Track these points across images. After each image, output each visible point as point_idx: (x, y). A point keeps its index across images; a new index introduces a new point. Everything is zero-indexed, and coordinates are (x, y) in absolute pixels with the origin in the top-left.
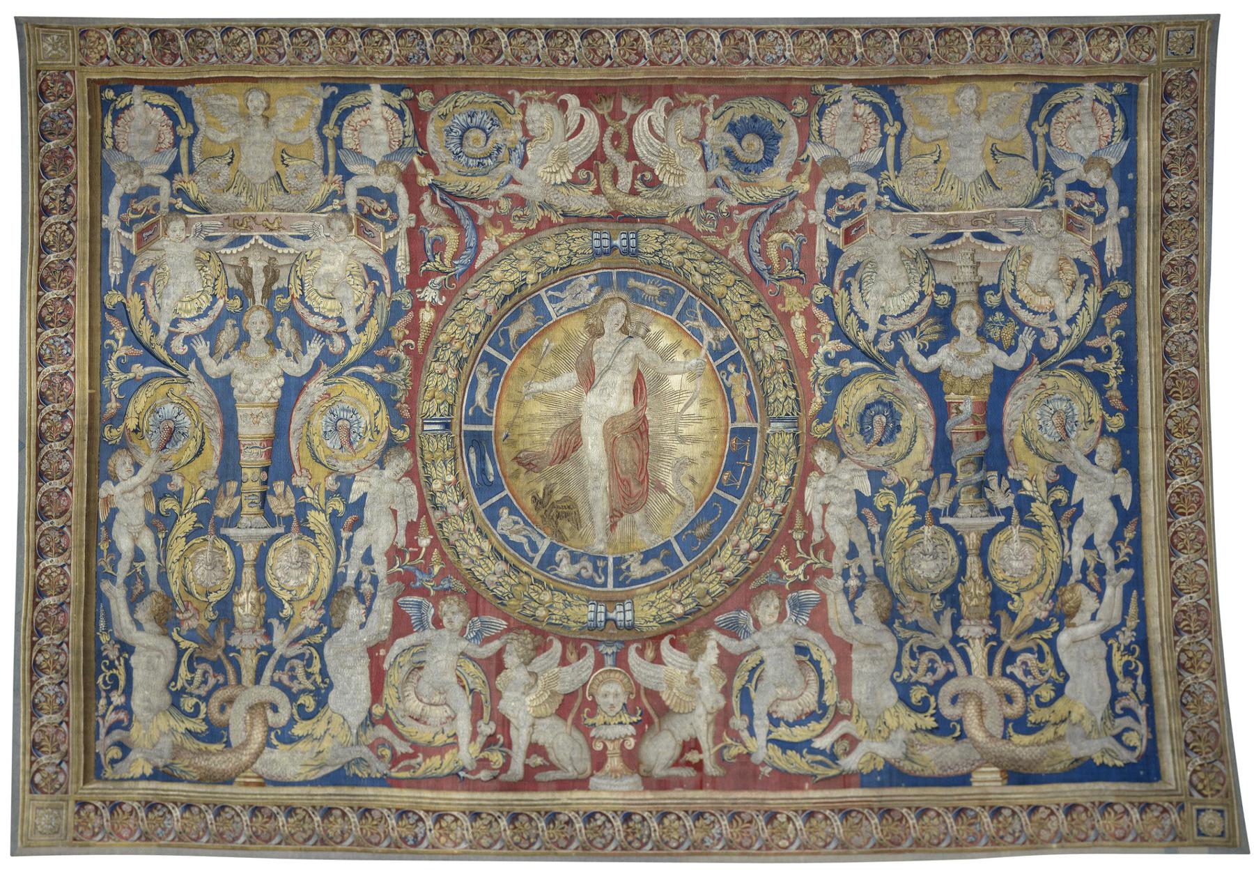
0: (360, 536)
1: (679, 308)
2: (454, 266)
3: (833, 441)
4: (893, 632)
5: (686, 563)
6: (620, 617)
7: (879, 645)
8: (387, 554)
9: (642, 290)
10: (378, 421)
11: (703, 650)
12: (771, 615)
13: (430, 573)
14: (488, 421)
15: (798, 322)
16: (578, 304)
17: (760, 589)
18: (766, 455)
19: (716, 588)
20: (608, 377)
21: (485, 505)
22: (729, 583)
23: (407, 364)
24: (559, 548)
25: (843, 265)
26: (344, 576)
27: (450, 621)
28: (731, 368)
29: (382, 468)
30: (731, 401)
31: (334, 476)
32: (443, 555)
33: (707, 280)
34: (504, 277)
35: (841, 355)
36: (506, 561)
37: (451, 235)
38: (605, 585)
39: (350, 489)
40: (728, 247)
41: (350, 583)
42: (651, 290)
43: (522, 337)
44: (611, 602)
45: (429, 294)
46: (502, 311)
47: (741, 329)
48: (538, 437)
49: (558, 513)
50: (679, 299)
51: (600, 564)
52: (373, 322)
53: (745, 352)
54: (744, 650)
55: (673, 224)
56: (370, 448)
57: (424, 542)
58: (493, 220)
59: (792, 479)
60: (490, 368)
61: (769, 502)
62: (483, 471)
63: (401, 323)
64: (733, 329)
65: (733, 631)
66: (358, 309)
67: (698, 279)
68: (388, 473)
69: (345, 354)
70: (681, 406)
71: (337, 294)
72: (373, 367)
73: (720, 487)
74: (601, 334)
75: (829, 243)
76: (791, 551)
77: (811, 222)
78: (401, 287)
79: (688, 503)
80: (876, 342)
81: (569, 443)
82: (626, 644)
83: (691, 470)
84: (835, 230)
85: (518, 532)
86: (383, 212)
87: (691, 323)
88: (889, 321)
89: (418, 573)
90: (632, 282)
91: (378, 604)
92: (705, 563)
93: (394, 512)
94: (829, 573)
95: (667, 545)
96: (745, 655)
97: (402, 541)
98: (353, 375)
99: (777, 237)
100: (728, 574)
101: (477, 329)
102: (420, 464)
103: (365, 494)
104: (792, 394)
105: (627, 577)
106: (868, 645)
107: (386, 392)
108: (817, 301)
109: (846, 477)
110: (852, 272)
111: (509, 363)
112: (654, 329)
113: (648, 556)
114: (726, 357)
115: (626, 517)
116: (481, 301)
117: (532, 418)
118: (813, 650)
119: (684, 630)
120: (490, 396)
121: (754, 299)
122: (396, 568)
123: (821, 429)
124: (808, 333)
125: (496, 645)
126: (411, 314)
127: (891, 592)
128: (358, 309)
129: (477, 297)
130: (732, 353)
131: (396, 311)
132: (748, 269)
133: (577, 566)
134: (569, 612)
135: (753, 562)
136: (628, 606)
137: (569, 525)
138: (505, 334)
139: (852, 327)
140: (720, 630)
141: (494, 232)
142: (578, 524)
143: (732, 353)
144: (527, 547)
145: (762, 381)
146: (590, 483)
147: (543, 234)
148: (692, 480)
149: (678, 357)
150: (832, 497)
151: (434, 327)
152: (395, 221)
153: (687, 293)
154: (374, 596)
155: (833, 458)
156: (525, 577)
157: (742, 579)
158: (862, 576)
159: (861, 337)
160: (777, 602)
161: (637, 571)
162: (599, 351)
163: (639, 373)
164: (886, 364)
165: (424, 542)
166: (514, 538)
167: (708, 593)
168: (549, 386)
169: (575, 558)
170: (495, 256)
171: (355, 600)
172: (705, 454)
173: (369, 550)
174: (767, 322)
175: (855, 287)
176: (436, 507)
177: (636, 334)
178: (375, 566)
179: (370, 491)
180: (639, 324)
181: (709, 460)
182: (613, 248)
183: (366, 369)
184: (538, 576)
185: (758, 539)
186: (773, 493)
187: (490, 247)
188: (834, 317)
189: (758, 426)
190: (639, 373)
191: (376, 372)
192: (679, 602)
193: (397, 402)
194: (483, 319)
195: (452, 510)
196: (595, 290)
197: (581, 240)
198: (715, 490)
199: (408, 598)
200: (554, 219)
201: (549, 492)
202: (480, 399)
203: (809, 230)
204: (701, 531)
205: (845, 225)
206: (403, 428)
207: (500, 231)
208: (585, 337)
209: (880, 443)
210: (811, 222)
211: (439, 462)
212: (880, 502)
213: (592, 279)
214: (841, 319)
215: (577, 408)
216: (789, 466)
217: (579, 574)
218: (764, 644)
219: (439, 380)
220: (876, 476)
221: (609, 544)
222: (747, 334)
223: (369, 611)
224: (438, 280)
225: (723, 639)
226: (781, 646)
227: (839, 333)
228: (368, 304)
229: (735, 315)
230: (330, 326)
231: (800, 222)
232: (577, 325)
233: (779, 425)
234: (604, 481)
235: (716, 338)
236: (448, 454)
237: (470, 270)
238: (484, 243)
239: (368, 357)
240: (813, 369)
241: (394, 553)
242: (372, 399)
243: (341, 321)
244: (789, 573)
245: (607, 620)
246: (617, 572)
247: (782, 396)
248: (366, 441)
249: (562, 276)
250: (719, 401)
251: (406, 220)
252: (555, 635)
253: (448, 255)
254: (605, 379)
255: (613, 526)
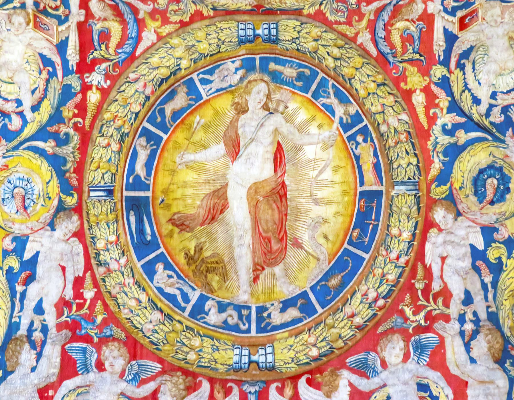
0: (34, 291)
1: (314, 87)
2: (117, 53)
3: (451, 200)
4: (505, 370)
5: (320, 310)
6: (262, 359)
7: (492, 382)
8: (56, 306)
9: (281, 73)
10: (50, 189)
11: (336, 388)
12: (397, 356)
13: (93, 321)
14: (146, 188)
15: (419, 99)
16: (224, 85)
17: (385, 333)
18: (390, 215)
19: (347, 333)
20: (252, 148)
21: (143, 262)
22: (359, 328)
23: (76, 139)
24: (208, 298)
25: (458, 49)
26: (17, 326)
27: (112, 365)
28: (360, 138)
29: (53, 229)
30: (360, 167)
31: (11, 237)
32: (106, 306)
33: (338, 63)
34: (160, 63)
35: (456, 127)
36: (161, 311)
37: (115, 28)
38: (248, 331)
39: (24, 249)
40: (357, 34)
41: (23, 331)
42: (290, 72)
43: (176, 115)
44: (254, 346)
45: (96, 78)
46: (158, 93)
47: (368, 105)
48: (189, 201)
49: (206, 268)
50: (312, 81)
51: (245, 312)
52: (46, 103)
53: (372, 124)
54: (373, 387)
55: (309, 16)
56: (42, 212)
57: (89, 294)
58: (152, 14)
59: (414, 235)
60: (148, 142)
61: (393, 256)
62: (141, 231)
63: (71, 103)
64: (361, 105)
65: (362, 370)
66: (33, 92)
67: (330, 62)
68: (59, 233)
69: (21, 130)
70: (316, 172)
71: (15, 79)
72: (45, 141)
73: (350, 243)
74: (245, 111)
75: (445, 30)
76: (415, 299)
77: (429, 11)
78: (71, 73)
79: (322, 257)
80: (488, 114)
81: (217, 208)
82: (268, 383)
83: (325, 229)
84: (451, 18)
85: (172, 285)
86: (57, 8)
87: (324, 100)
88: (499, 96)
89: (83, 322)
90: (272, 66)
91: (48, 349)
92: (337, 310)
93: (63, 269)
94: (447, 319)
95: (304, 295)
96: (372, 392)
97: (69, 294)
98: (28, 148)
99: (400, 25)
100: (358, 320)
101: (136, 108)
102: (86, 226)
103: (38, 253)
104: (414, 161)
105: (269, 324)
106: (482, 382)
107: (56, 162)
108: (435, 79)
109: (462, 233)
110: (466, 54)
111: (165, 137)
112: (292, 105)
113: (286, 305)
114: (356, 128)
115: (267, 270)
116: (141, 84)
117: (185, 185)
118: (433, 387)
119: (320, 370)
120: (148, 165)
121: (380, 78)
122: (64, 319)
123: (439, 192)
124: (427, 108)
125: (151, 386)
126: (80, 96)
127: (503, 335)
128: (33, 92)
129: (137, 80)
130: (360, 126)
131: (66, 93)
132: (374, 52)
133: (224, 315)
134: (216, 355)
135: (381, 309)
136: (269, 350)
137: (217, 278)
138: (162, 112)
139: (466, 102)
140: (352, 370)
141: (152, 25)
142: (225, 277)
143: (360, 126)
144: (179, 298)
145: (386, 150)
146: (235, 243)
147: (195, 25)
148: (326, 237)
149: (313, 129)
150: (451, 252)
151: (99, 108)
152: (67, 17)
153: (321, 75)
154: (44, 343)
155: (450, 217)
156: (178, 325)
157: (370, 324)
158: (477, 321)
159: (474, 111)
160: (402, 344)
161: (277, 318)
162: (243, 126)
163: (279, 144)
164: (497, 134)
165: (89, 294)
166: (168, 290)
167: (340, 337)
168: (200, 156)
169: (222, 308)
170: (154, 44)
171: (27, 346)
172: (337, 214)
173: (41, 301)
174: (391, 99)
175: (469, 68)
176: (100, 264)
177: (276, 110)
178: (46, 316)
179: (42, 250)
180: (279, 102)
181: (340, 219)
182: (256, 36)
183: (40, 144)
184: (189, 324)
185: (384, 289)
186: (397, 248)
187: (149, 37)
188: (450, 93)
189: (383, 188)
190: (279, 144)
191: (49, 146)
192: (314, 345)
193: (65, 172)
194: (142, 99)
195: (114, 266)
196: (241, 73)
197: (229, 30)
198: (346, 245)
199: (74, 344)
200: (205, 13)
201: (199, 249)
202: (140, 169)
203: (427, 19)
204: (334, 282)
205: (460, 14)
206: (72, 195)
207: (159, 23)
208: (231, 114)
209: (492, 203)
210: (429, 11)
211: (103, 224)
212: (492, 255)
213: (238, 64)
214: (457, 96)
215: (224, 176)
216: (412, 224)
217: (225, 322)
218: (389, 383)
219: (103, 153)
220: (488, 232)
221: (252, 295)
222: (373, 109)
223: (39, 356)
224: (104, 65)
225: (355, 379)
226: (406, 383)
227: (454, 107)
228: (42, 87)
229: (362, 93)
230: (10, 107)
231: (420, 12)
232: (225, 103)
233: (403, 188)
234: (248, 239)
235: (346, 113)
236: (111, 217)
237: (132, 58)
238: (144, 34)
239: (41, 134)
240: (432, 139)
241: (63, 304)
242: (45, 169)
243: (19, 102)
244: (412, 318)
245: (250, 362)
246: (260, 319)
247: (405, 162)
248: (39, 206)
249: (212, 63)
250: (349, 167)
251: (77, 15)
252: (204, 376)
253: (114, 42)
254: (249, 150)
255: (256, 279)
